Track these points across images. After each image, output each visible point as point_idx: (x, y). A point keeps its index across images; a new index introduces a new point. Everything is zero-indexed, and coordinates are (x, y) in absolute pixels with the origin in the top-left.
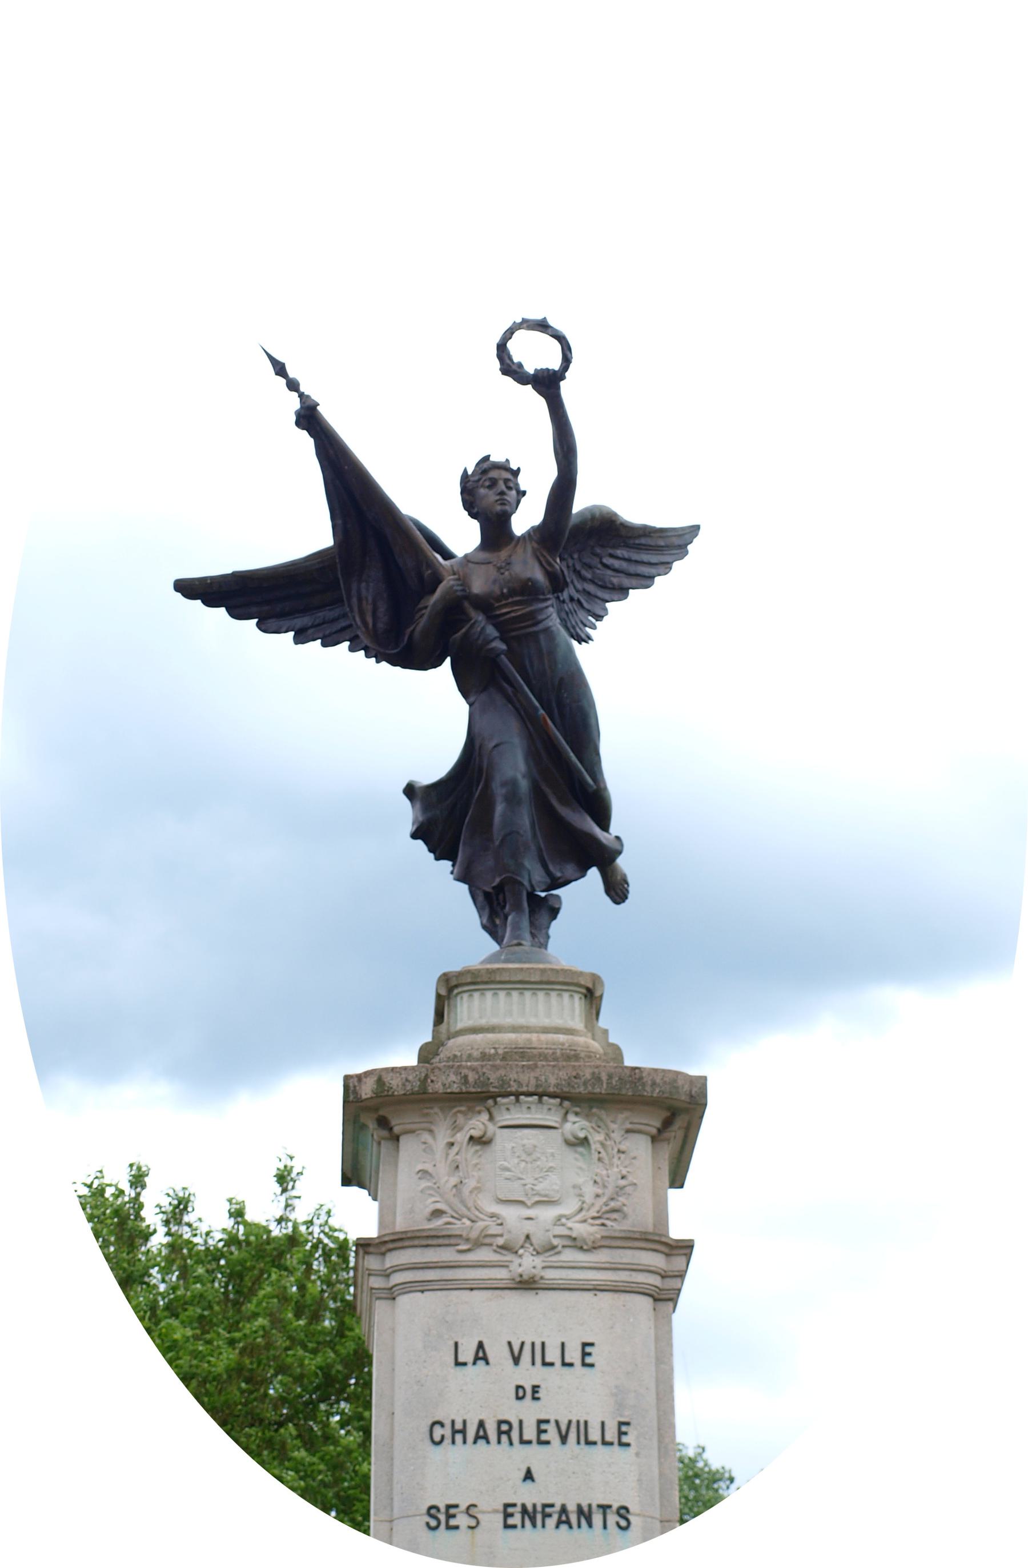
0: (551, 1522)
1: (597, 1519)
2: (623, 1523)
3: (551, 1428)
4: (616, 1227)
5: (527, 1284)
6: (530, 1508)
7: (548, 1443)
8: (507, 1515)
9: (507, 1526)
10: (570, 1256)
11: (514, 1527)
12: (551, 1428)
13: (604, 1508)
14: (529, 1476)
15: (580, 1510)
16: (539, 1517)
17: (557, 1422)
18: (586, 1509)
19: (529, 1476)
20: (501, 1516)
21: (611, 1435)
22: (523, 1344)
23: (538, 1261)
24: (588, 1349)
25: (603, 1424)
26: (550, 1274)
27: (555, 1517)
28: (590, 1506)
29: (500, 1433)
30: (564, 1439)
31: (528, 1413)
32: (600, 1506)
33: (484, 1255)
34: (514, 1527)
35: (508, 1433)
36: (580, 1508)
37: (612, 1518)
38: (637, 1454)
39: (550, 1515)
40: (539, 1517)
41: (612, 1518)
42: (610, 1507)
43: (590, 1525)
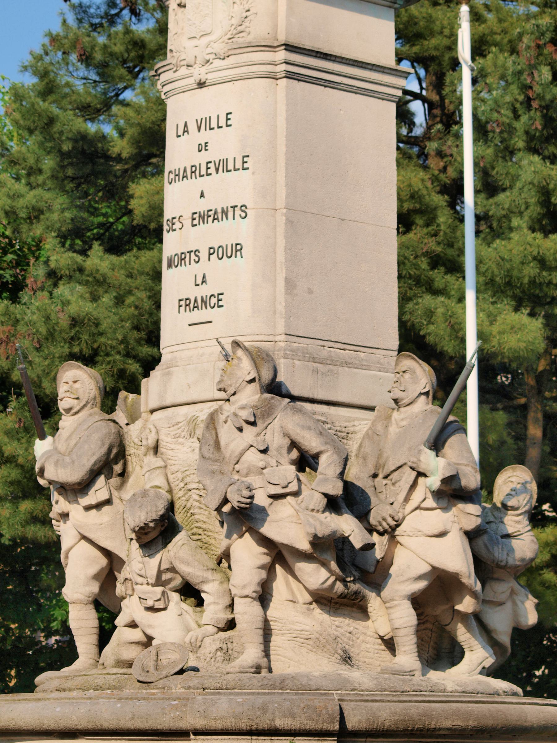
0: (210, 219)
1: (230, 214)
2: (243, 215)
3: (211, 165)
4: (240, 40)
5: (201, 85)
6: (202, 214)
7: (210, 174)
8: (194, 219)
9: (194, 226)
10: (218, 63)
11: (196, 225)
12: (211, 165)
13: (234, 207)
14: (202, 195)
15: (223, 211)
16: (206, 217)
17: (215, 162)
18: (225, 210)
19: (202, 195)
20: (191, 220)
21: (239, 165)
22: (202, 119)
23: (204, 70)
24: (229, 116)
25: (235, 158)
26: (210, 76)
27: (212, 216)
28: (227, 208)
29: (192, 172)
30: (217, 170)
31: (201, 159)
32: (232, 207)
33: (183, 71)
34: (196, 225)
35: (195, 172)
36: (223, 209)
37: (238, 212)
38: (253, 173)
39: (210, 216)
40: (206, 217)
41: (238, 212)
42: (236, 206)
43: (227, 218)
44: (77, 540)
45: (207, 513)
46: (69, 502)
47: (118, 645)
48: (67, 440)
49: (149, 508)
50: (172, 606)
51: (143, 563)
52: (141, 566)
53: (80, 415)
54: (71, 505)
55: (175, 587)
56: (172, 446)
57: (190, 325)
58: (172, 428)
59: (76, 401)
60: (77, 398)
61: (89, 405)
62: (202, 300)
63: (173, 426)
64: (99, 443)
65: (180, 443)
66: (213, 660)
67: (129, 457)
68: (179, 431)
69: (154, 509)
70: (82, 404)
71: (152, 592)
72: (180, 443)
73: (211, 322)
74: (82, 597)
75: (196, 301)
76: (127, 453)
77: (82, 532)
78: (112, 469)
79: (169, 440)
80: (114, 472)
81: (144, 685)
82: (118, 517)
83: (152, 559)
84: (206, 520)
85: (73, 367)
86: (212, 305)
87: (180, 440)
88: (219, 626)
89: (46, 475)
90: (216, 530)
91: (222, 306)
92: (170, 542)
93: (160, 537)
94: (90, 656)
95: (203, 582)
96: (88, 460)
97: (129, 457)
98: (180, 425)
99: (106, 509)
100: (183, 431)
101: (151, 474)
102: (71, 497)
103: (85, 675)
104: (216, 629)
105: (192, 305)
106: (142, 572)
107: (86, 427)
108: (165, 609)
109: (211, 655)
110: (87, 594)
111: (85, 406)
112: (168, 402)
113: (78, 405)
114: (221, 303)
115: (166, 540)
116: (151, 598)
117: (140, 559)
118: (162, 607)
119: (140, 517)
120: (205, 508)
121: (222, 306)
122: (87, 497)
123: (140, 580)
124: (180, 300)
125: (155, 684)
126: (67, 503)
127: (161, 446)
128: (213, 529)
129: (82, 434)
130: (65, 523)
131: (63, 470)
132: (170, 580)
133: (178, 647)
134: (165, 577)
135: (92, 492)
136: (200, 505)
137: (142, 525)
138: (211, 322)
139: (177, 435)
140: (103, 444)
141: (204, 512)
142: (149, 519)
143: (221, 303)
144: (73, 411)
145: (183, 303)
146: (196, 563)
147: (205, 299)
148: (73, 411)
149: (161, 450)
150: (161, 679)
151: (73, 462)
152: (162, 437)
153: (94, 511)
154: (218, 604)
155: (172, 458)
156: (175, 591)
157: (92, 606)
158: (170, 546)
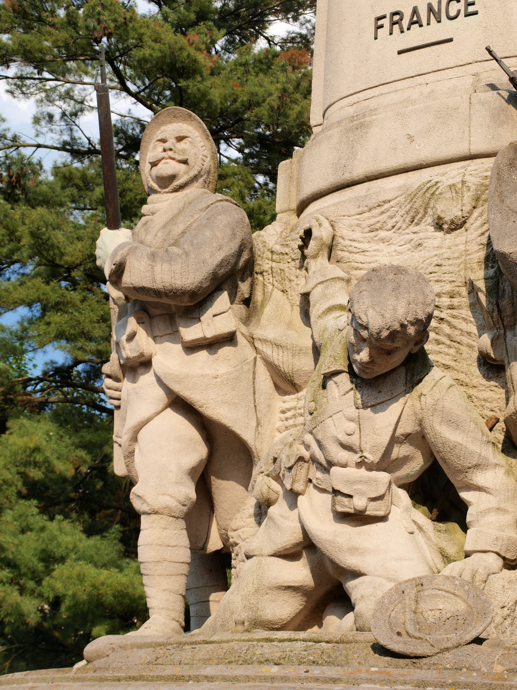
44: (161, 407)
45: (452, 351)
46: (154, 338)
47: (257, 591)
48: (165, 227)
49: (413, 295)
50: (396, 514)
51: (358, 421)
52: (352, 426)
53: (187, 191)
54: (158, 346)
55: (408, 476)
56: (364, 246)
57: (400, 53)
58: (366, 215)
59: (183, 166)
60: (185, 162)
61: (201, 180)
62: (430, 9)
63: (370, 210)
64: (229, 232)
65: (383, 240)
66: (509, 621)
67: (260, 277)
68: (385, 216)
69: (421, 298)
70: (192, 174)
71: (366, 482)
72: (383, 240)
73: (450, 40)
74: (172, 503)
75: (415, 11)
76: (257, 269)
77: (176, 388)
78: (236, 287)
79: (357, 235)
80: (239, 294)
81: (401, 661)
82: (246, 368)
83: (380, 414)
84: (452, 364)
85: (175, 117)
86: (452, 14)
87: (382, 234)
88: (508, 556)
89: (127, 279)
90: (475, 382)
91: (476, 13)
92: (420, 381)
93: (403, 369)
94: (174, 615)
95: (477, 466)
96: (212, 255)
97: (260, 277)
98: (387, 206)
99: (226, 351)
100: (391, 217)
101: (326, 288)
102: (160, 327)
103: (207, 642)
104: (500, 562)
105: (405, 23)
106: (354, 440)
107: (204, 205)
108: (383, 519)
109: (506, 611)
110: (182, 498)
111: (195, 178)
112: (358, 172)
113: (185, 173)
114: (471, 9)
115: (413, 375)
116: (362, 494)
117: (352, 412)
118: (381, 513)
119: (395, 310)
120: (448, 342)
121: (476, 13)
122: (198, 326)
123: (343, 455)
124: (379, 19)
125: (434, 659)
126: (150, 340)
127: (340, 247)
128: (467, 380)
129: (196, 216)
130: (134, 381)
131: (166, 266)
132: (405, 460)
133: (462, 585)
134: (399, 451)
135: (207, 316)
136: (438, 337)
137: (397, 326)
138: (450, 40)
139: (378, 225)
140: (234, 235)
141: (446, 350)
142: (410, 318)
143: (471, 9)
144: (176, 183)
145: (386, 22)
146: (472, 425)
147: (436, 9)
148: (176, 183)
149: (338, 253)
150: (447, 649)
151: (187, 254)
152: (343, 230)
153: (203, 354)
154: (505, 511)
155: (361, 266)
156: (400, 487)
157: (182, 524)
158: (421, 388)
